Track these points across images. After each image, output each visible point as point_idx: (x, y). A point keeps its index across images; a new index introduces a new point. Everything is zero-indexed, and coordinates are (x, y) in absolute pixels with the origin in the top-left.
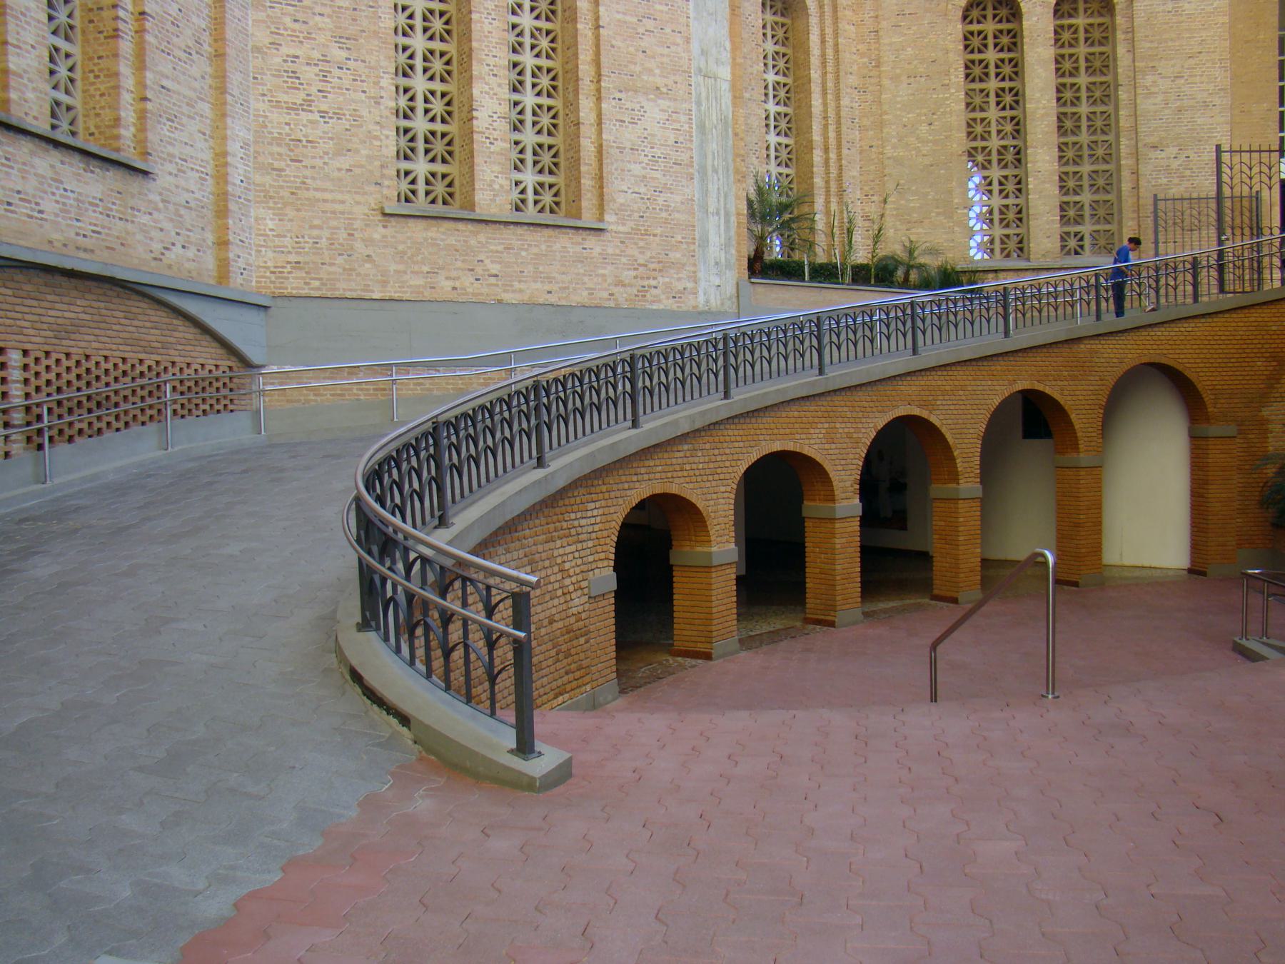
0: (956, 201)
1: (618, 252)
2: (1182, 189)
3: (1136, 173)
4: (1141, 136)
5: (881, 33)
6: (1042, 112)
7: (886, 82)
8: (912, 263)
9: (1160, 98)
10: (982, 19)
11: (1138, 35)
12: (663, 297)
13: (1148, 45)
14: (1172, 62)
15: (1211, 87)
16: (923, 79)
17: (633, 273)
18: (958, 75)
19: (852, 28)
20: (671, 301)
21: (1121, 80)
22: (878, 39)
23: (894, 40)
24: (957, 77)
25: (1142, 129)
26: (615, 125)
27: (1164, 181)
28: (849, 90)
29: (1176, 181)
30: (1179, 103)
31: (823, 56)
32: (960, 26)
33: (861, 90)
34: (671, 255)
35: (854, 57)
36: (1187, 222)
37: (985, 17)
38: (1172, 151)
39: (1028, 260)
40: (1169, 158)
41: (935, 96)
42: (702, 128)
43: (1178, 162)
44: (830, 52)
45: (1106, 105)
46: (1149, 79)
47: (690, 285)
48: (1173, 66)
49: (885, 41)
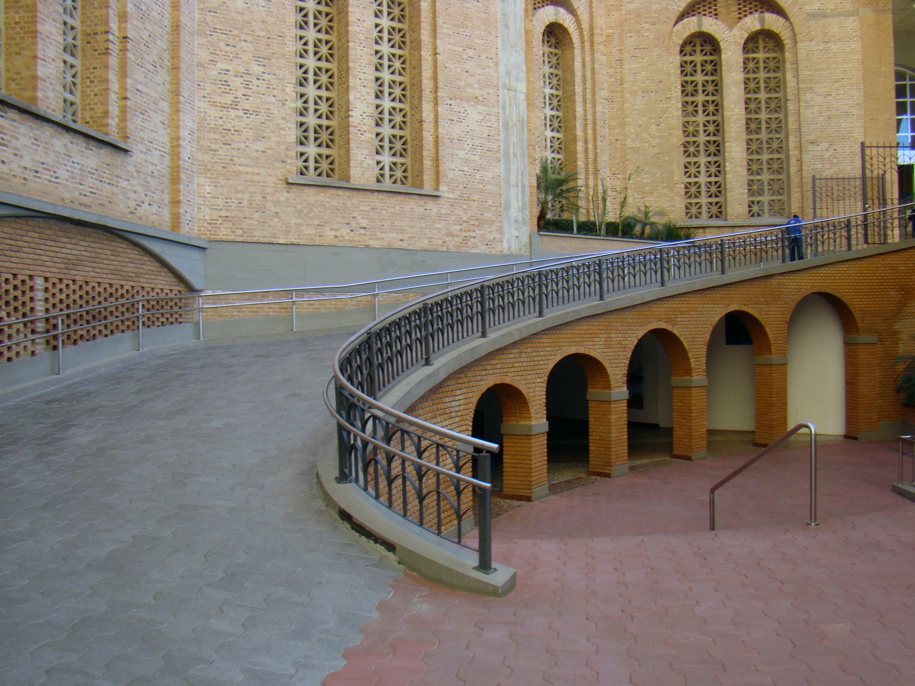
0: (676, 178)
1: (448, 212)
3: (800, 160)
4: (803, 135)
5: (623, 61)
6: (735, 117)
7: (627, 95)
8: (647, 221)
9: (816, 109)
10: (693, 53)
11: (801, 67)
12: (479, 244)
13: (808, 73)
14: (824, 85)
15: (850, 102)
16: (653, 94)
17: (459, 227)
18: (677, 92)
19: (604, 57)
20: (485, 247)
21: (790, 96)
22: (621, 65)
24: (676, 92)
25: (804, 130)
26: (447, 123)
27: (819, 166)
28: (602, 101)
29: (828, 166)
30: (828, 113)
31: (584, 76)
32: (678, 58)
33: (610, 100)
34: (485, 215)
35: (605, 77)
36: (835, 195)
37: (695, 51)
38: (824, 145)
39: (726, 220)
40: (823, 150)
42: (506, 127)
43: (830, 153)
44: (588, 74)
45: (779, 113)
46: (809, 96)
47: (498, 236)
48: (825, 87)
49: (626, 67)
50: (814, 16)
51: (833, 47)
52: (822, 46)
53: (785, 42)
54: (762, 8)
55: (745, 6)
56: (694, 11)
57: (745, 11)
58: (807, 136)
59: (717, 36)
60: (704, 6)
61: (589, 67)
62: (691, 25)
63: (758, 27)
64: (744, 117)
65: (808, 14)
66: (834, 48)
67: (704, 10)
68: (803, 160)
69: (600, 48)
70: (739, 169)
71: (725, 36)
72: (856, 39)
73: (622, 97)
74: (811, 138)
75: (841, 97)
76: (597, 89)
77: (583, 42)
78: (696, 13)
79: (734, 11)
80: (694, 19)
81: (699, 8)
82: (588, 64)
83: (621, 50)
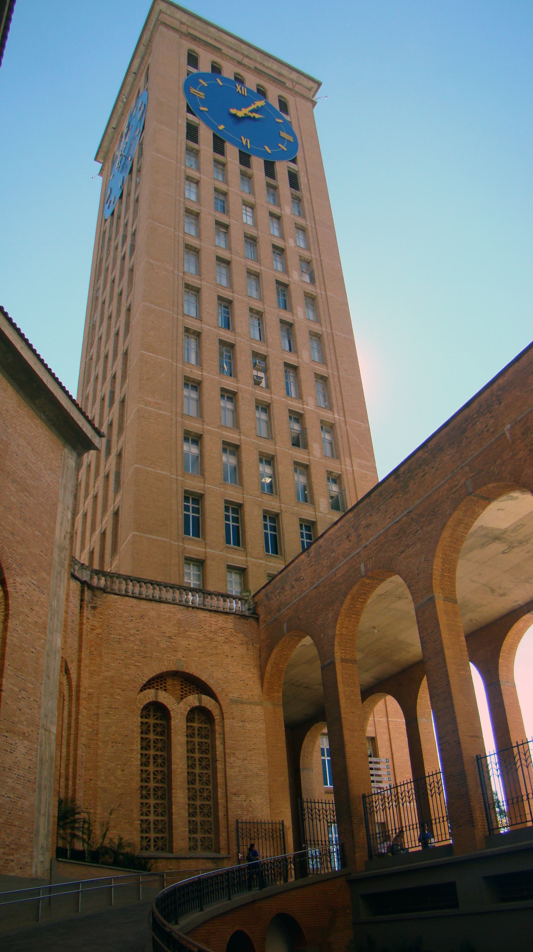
2: (248, 817)
4: (229, 788)
6: (180, 770)
7: (100, 744)
9: (237, 769)
10: (148, 716)
11: (227, 736)
13: (231, 742)
16: (120, 745)
18: (137, 746)
22: (98, 719)
23: (105, 721)
24: (137, 746)
25: (229, 784)
26: (3, 752)
27: (240, 812)
29: (246, 813)
30: (245, 773)
31: (69, 723)
35: (86, 727)
37: (149, 715)
38: (243, 797)
39: (172, 852)
40: (242, 801)
41: (126, 755)
42: (41, 761)
44: (73, 722)
46: (232, 759)
48: (243, 754)
50: (234, 702)
51: (248, 725)
52: (240, 724)
53: (215, 718)
54: (197, 690)
55: (186, 687)
56: (150, 685)
57: (186, 691)
58: (231, 790)
59: (168, 707)
60: (158, 682)
61: (73, 718)
62: (150, 695)
63: (197, 704)
64: (186, 771)
65: (231, 700)
66: (248, 726)
67: (157, 686)
68: (229, 807)
69: (83, 702)
70: (182, 811)
71: (174, 707)
72: (262, 721)
73: (97, 744)
74: (234, 790)
75: (254, 762)
76: (79, 735)
77: (70, 696)
78: (151, 686)
79: (178, 690)
80: (153, 691)
81: (154, 683)
82: (73, 714)
83: (98, 707)
